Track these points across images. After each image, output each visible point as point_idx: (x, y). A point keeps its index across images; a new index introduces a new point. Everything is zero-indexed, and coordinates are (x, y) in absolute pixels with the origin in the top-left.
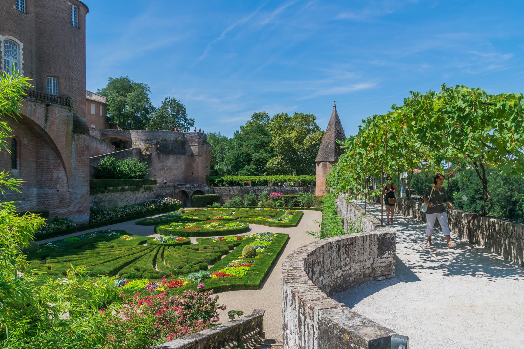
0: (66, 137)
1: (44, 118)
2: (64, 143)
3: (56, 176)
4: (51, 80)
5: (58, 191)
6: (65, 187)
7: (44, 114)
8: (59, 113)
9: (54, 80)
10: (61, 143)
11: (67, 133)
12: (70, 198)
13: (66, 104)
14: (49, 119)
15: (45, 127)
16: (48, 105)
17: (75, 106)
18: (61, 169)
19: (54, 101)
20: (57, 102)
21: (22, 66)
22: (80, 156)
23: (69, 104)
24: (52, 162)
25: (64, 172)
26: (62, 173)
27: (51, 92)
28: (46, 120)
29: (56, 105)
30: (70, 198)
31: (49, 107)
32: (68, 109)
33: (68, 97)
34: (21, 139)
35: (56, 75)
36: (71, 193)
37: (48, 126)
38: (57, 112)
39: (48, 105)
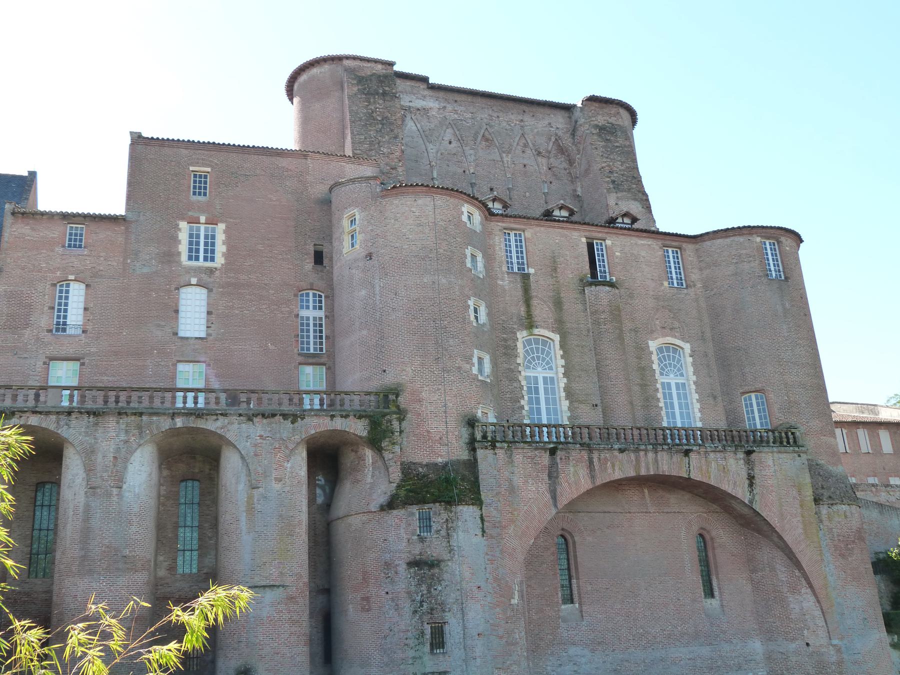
0: (802, 516)
1: (747, 482)
2: (800, 531)
3: (797, 610)
4: (750, 399)
5: (808, 644)
6: (822, 633)
7: (744, 474)
8: (774, 464)
9: (757, 398)
10: (792, 531)
11: (801, 506)
12: (840, 663)
13: (788, 442)
14: (757, 481)
15: (751, 501)
16: (749, 453)
17: (810, 442)
18: (805, 590)
19: (762, 441)
20: (768, 442)
21: (693, 387)
22: (842, 556)
23: (795, 442)
24: (783, 577)
25: (812, 599)
26: (808, 602)
27: (755, 424)
28: (751, 485)
29: (766, 449)
30: (840, 663)
31: (753, 456)
32: (794, 452)
33: (791, 427)
34: (714, 533)
35: (759, 386)
36: (839, 650)
37: (757, 498)
38: (770, 463)
39: (749, 453)
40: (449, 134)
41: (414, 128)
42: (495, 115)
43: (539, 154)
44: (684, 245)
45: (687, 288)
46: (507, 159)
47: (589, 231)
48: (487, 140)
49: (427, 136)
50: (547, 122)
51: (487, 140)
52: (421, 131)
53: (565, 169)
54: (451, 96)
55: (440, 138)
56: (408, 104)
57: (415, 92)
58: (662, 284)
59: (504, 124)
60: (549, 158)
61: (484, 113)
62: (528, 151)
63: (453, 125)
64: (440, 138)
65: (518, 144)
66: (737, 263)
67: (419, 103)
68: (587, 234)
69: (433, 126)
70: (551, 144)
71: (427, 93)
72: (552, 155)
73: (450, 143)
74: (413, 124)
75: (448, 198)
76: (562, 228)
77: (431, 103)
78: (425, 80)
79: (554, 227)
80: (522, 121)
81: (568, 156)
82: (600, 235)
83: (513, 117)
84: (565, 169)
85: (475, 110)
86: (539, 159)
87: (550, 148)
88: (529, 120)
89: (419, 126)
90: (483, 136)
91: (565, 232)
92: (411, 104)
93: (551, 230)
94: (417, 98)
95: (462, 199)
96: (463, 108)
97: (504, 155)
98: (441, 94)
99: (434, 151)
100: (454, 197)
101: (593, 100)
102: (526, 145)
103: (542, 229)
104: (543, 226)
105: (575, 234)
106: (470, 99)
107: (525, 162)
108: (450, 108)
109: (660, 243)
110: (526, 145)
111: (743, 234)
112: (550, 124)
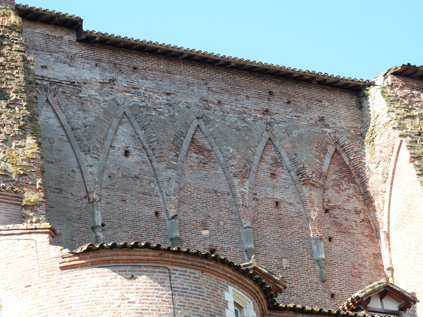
40: (124, 137)
41: (53, 121)
42: (214, 98)
46: (243, 189)
48: (200, 150)
50: (315, 115)
51: (200, 150)
53: (357, 212)
54: (126, 60)
57: (53, 47)
59: (233, 118)
60: (324, 189)
62: (283, 175)
63: (136, 116)
64: (107, 144)
67: (60, 72)
69: (91, 119)
70: (327, 161)
71: (77, 50)
72: (329, 183)
73: (127, 153)
74: (51, 114)
75: (198, 274)
77: (87, 71)
78: (73, 25)
83: (248, 104)
84: (357, 212)
85: (172, 89)
87: (325, 169)
89: (62, 117)
90: (193, 141)
92: (45, 73)
94: (57, 60)
95: (224, 276)
96: (148, 84)
97: (236, 181)
98: (105, 55)
99: (94, 170)
100: (210, 271)
102: (277, 163)
106: (163, 65)
107: (278, 196)
108: (122, 81)
110: (277, 163)
112: (322, 119)
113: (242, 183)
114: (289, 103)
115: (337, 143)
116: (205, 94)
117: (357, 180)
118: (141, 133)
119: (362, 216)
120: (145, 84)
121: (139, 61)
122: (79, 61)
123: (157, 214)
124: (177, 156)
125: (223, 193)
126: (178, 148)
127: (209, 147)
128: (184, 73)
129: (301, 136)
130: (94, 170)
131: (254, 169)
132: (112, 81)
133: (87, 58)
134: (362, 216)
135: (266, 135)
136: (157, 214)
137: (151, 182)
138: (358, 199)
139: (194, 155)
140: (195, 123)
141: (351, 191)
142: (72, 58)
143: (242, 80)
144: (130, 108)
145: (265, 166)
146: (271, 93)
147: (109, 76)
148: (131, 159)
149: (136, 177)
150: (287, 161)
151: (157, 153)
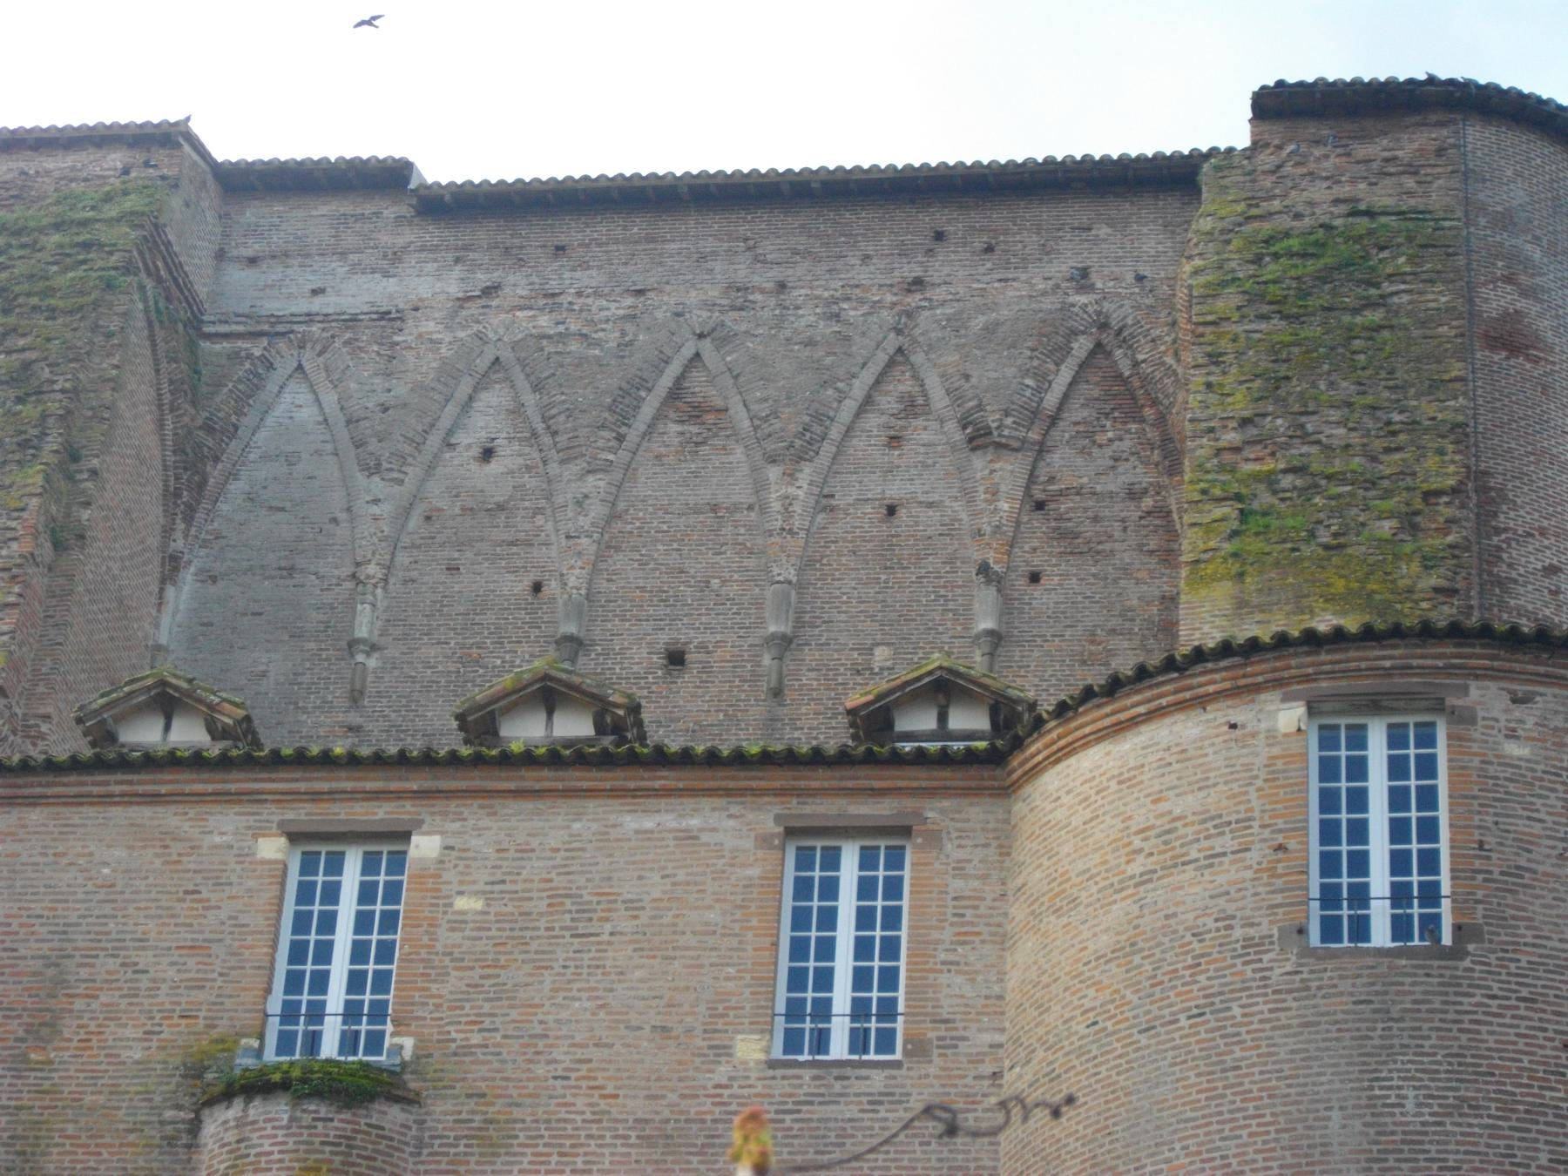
40: (488, 417)
41: (308, 414)
42: (765, 278)
43: (979, 438)
44: (935, 811)
45: (918, 1049)
47: (315, 797)
48: (697, 412)
49: (366, 444)
50: (1061, 268)
51: (697, 412)
52: (338, 419)
53: (1133, 494)
54: (534, 235)
55: (435, 440)
56: (303, 306)
57: (350, 240)
58: (724, 1051)
60: (1042, 449)
61: (691, 280)
62: (922, 433)
64: (435, 440)
65: (868, 401)
66: (1146, 878)
67: (358, 292)
68: (301, 814)
69: (401, 390)
73: (487, 454)
74: (304, 397)
76: (154, 799)
77: (429, 283)
78: (388, 178)
79: (106, 800)
80: (918, 283)
81: (1161, 420)
82: (381, 813)
83: (862, 275)
86: (979, 462)
87: (1051, 400)
88: (957, 275)
89: (330, 398)
90: (676, 393)
91: (169, 818)
92: (317, 304)
93: (75, 815)
94: (356, 269)
96: (590, 278)
97: (774, 472)
98: (483, 233)
99: (385, 509)
101: (1278, 105)
103: (35, 816)
104: (34, 801)
105: (225, 825)
106: (638, 226)
107: (895, 490)
108: (518, 284)
109: (765, 818)
111: (1202, 702)
113: (791, 476)
114: (989, 249)
115: (1104, 326)
116: (741, 271)
117: (1148, 412)
118: (530, 399)
119: (1148, 503)
120: (568, 279)
121: (571, 231)
122: (412, 260)
123: (537, 588)
124: (620, 438)
125: (735, 508)
126: (625, 420)
127: (719, 403)
128: (687, 235)
129: (990, 330)
130: (385, 509)
131: (835, 433)
132: (490, 291)
133: (435, 249)
134: (1148, 503)
135: (893, 342)
136: (537, 588)
137: (538, 511)
138: (1145, 462)
139: (674, 428)
140: (688, 352)
141: (1126, 444)
142: (396, 256)
143: (860, 219)
144: (514, 346)
145: (873, 421)
146: (939, 236)
147: (482, 279)
148: (494, 467)
149: (501, 507)
150: (939, 398)
151: (562, 439)
